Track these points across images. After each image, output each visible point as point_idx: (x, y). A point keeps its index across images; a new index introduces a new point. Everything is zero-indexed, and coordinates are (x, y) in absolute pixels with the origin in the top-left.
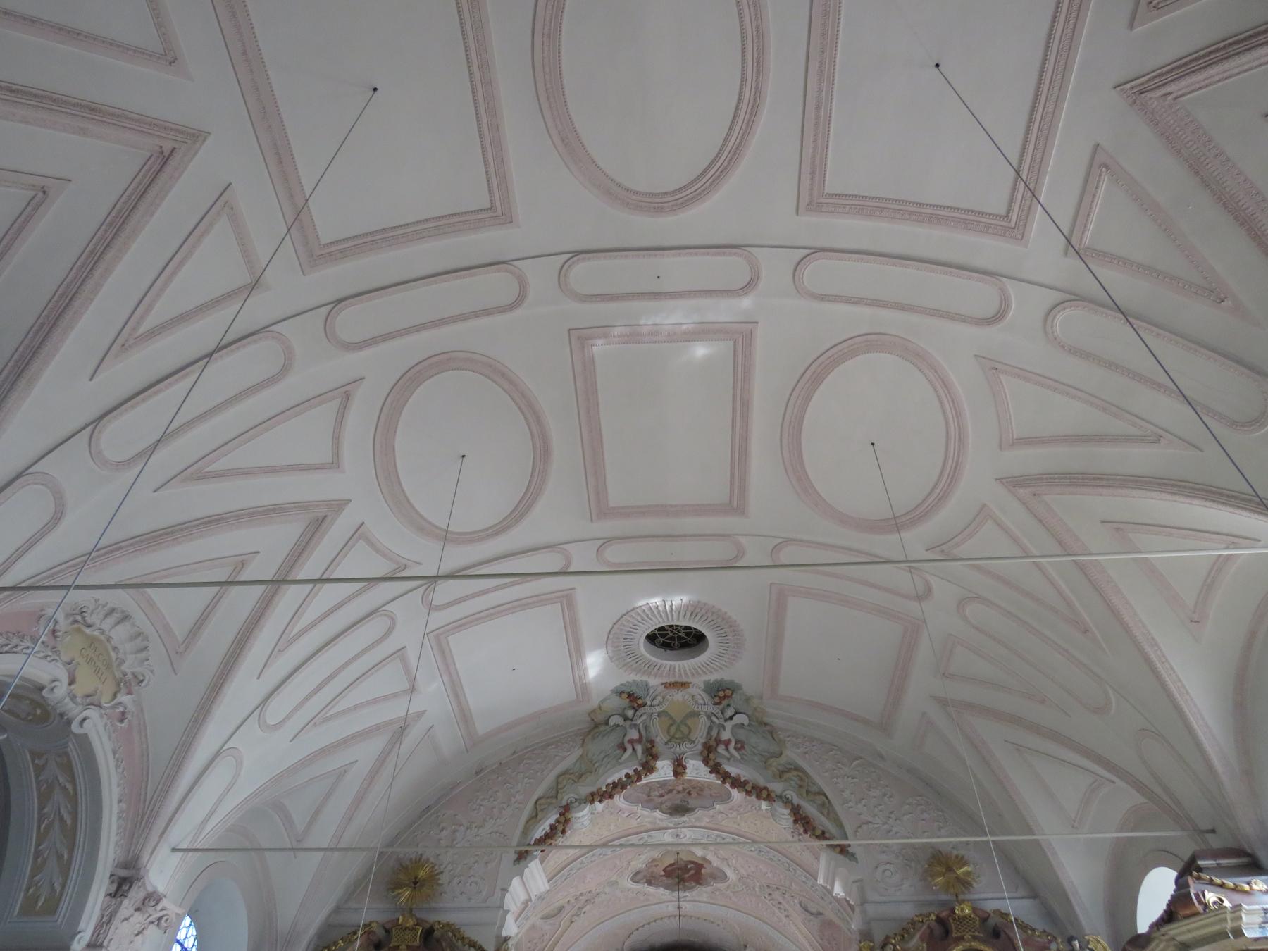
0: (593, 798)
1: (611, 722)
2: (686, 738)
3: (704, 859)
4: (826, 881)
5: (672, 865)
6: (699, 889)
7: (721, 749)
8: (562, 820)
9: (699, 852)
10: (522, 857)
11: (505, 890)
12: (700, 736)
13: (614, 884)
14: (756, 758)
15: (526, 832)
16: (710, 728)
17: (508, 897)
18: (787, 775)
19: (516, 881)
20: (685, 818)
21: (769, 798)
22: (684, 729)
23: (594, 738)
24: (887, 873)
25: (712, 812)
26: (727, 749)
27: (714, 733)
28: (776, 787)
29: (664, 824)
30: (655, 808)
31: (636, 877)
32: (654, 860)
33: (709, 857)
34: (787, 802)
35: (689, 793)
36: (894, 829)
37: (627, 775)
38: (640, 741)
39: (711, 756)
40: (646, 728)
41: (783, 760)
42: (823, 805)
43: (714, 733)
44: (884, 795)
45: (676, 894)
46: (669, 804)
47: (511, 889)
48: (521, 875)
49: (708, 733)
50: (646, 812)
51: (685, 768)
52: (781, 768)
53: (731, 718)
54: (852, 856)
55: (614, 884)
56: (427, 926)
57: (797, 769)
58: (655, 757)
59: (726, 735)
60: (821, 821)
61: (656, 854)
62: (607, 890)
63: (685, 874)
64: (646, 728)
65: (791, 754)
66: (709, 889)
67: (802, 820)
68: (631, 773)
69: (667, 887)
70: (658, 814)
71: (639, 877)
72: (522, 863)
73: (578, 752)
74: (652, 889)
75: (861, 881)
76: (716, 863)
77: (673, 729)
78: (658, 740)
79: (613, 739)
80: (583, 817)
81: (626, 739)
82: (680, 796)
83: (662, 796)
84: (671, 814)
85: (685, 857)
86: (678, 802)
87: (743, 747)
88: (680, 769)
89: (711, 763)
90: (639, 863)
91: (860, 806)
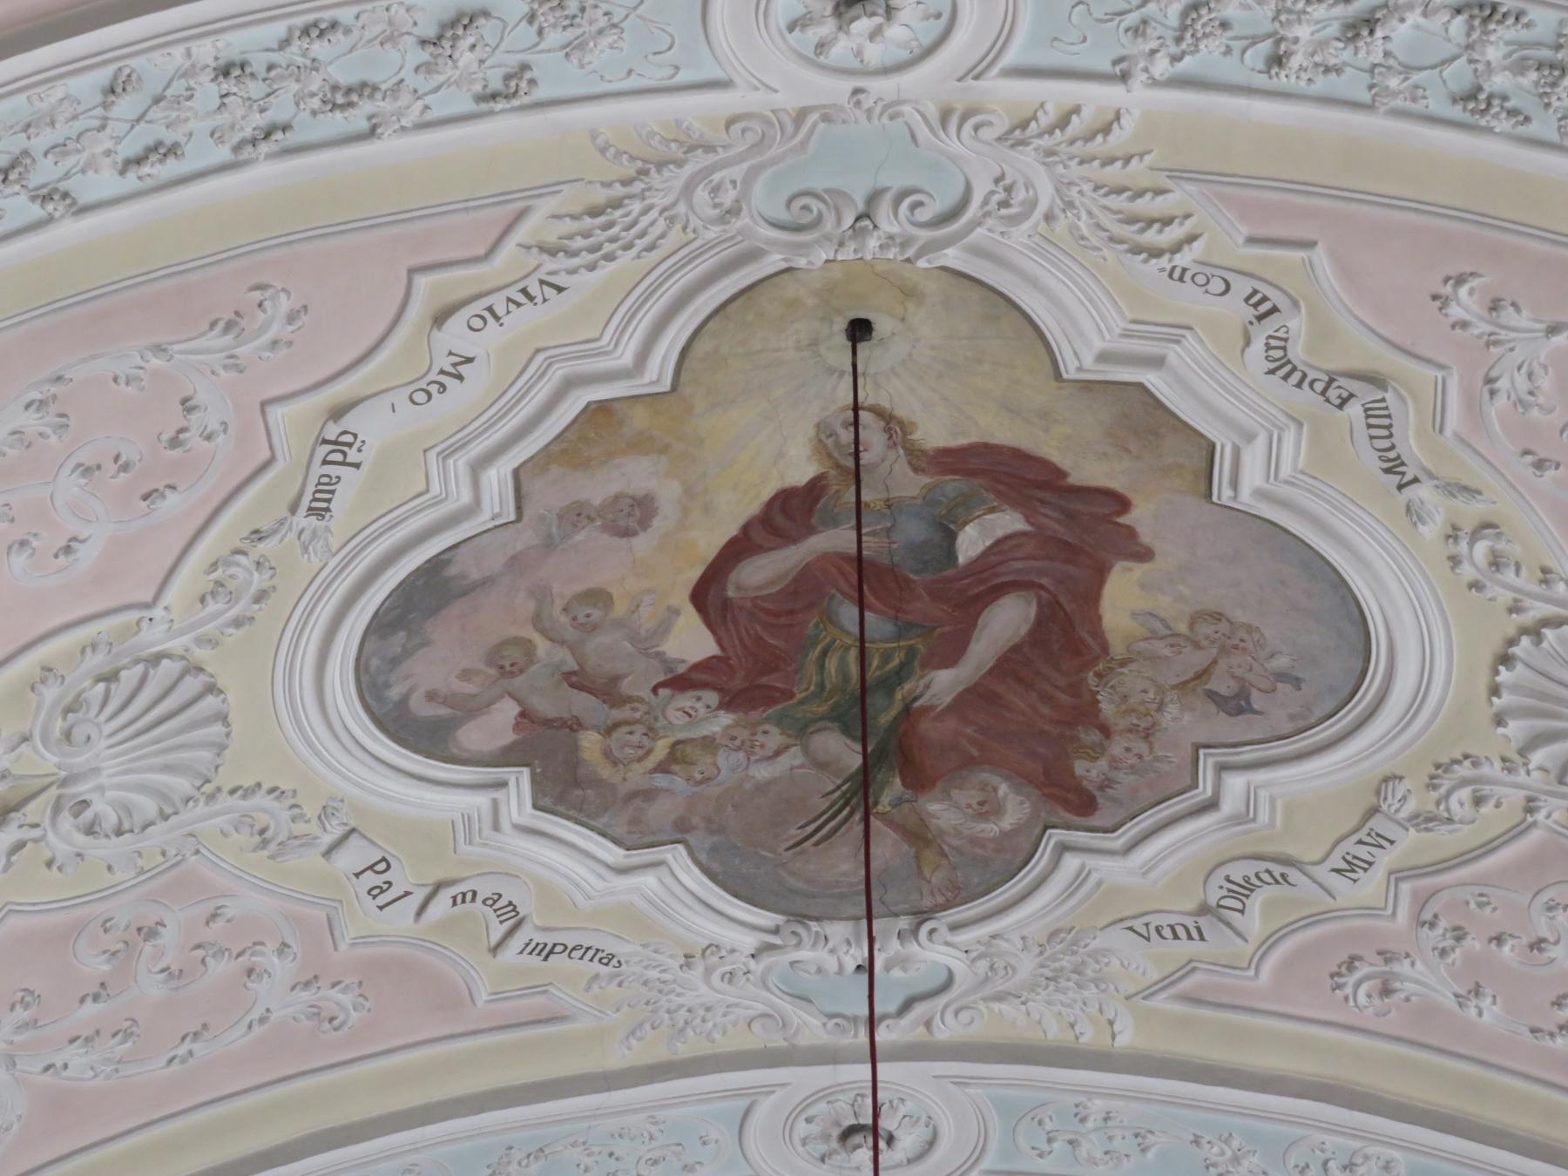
3: (1143, 418)
5: (790, 512)
9: (1087, 322)
13: (175, 698)
33: (1207, 383)
45: (834, 949)
55: (175, 698)
61: (620, 336)
62: (113, 773)
66: (1153, 862)
71: (436, 668)
74: (569, 865)
76: (1271, 458)
90: (440, 467)
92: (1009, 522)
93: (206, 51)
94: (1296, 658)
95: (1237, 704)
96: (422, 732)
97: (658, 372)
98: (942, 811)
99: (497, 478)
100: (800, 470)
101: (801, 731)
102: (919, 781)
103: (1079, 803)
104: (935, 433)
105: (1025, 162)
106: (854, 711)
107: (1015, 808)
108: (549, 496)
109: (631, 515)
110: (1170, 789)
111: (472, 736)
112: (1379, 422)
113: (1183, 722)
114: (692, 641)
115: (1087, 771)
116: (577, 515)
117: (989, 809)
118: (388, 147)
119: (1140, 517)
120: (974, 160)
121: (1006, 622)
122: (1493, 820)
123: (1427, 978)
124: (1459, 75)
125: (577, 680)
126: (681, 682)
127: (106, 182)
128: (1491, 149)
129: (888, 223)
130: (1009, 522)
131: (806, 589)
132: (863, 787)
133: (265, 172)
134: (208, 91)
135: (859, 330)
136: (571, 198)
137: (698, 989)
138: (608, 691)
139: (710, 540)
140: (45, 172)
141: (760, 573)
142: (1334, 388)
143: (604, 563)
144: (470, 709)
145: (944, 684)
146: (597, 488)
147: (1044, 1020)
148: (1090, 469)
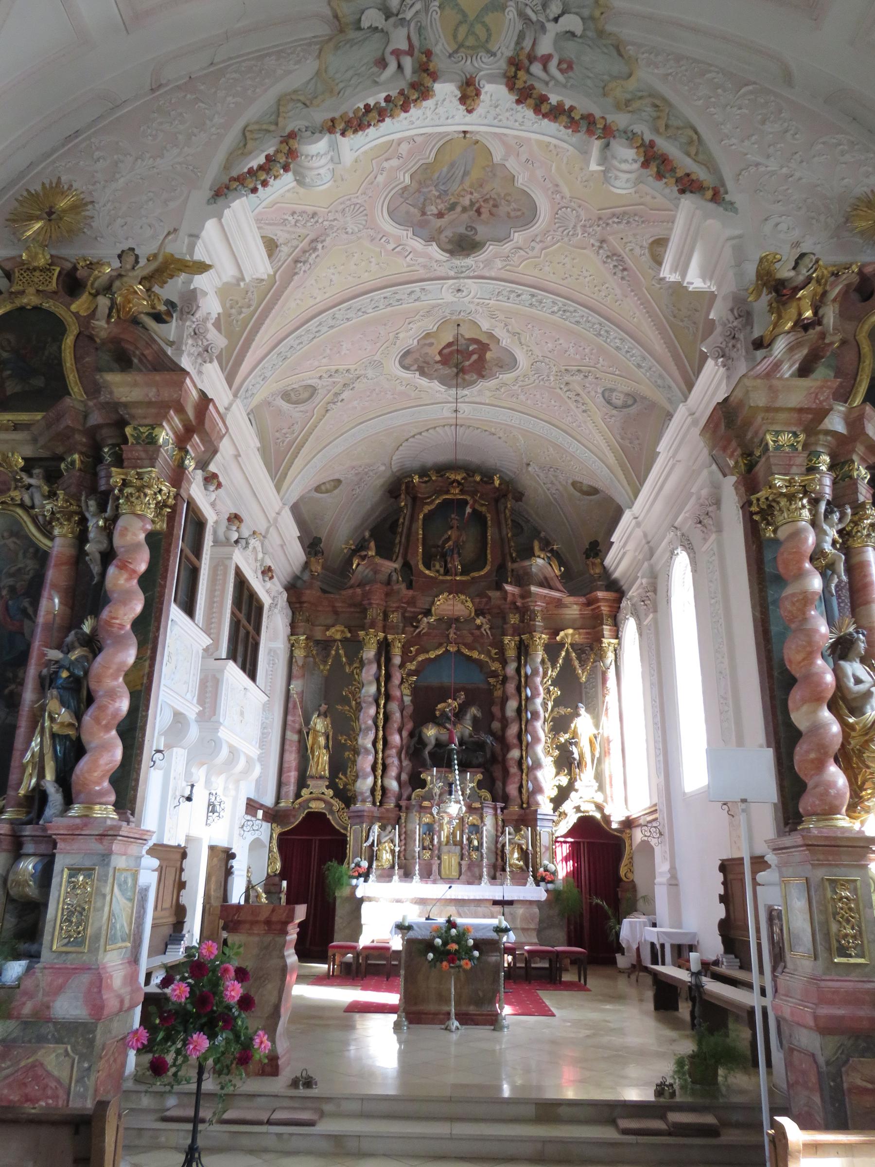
0: (330, 127)
1: (365, 24)
2: (483, 46)
3: (491, 336)
4: (674, 269)
5: (450, 345)
6: (482, 384)
7: (536, 69)
8: (285, 149)
9: (485, 325)
10: (222, 192)
11: (195, 237)
12: (505, 46)
14: (589, 82)
15: (227, 165)
16: (521, 36)
17: (200, 243)
18: (636, 105)
19: (211, 227)
20: (469, 261)
21: (608, 133)
22: (479, 29)
23: (337, 48)
24: (783, 227)
25: (507, 247)
26: (545, 69)
27: (527, 44)
28: (620, 120)
29: (442, 271)
30: (430, 239)
31: (407, 360)
32: (428, 335)
33: (498, 333)
34: (631, 137)
35: (479, 212)
36: (797, 175)
37: (388, 99)
38: (410, 52)
39: (521, 74)
40: (420, 30)
41: (632, 84)
42: (691, 142)
43: (527, 44)
44: (786, 131)
45: (453, 391)
46: (449, 233)
47: (204, 234)
48: (220, 216)
49: (518, 43)
50: (417, 244)
51: (478, 94)
52: (629, 96)
53: (556, 20)
54: (731, 206)
56: (69, 266)
57: (653, 94)
58: (434, 76)
59: (545, 46)
60: (685, 163)
62: (370, 373)
63: (464, 359)
64: (420, 30)
65: (647, 76)
66: (492, 383)
67: (654, 160)
68: (394, 93)
69: (443, 382)
70: (434, 250)
71: (408, 361)
72: (221, 201)
73: (310, 66)
74: (424, 382)
75: (740, 237)
76: (506, 341)
77: (463, 30)
78: (437, 50)
79: (371, 49)
80: (317, 150)
81: (390, 49)
82: (465, 216)
83: (440, 215)
84: (451, 252)
85: (467, 333)
86: (462, 230)
87: (570, 67)
88: (470, 91)
89: (519, 84)
90: (409, 339)
91: (746, 143)
92: (475, 346)
93: (382, 296)
94: (508, 363)
95: (501, 367)
96: (406, 368)
97: (435, 329)
98: (467, 377)
99: (415, 341)
100: (451, 340)
101: (450, 368)
102: (464, 373)
103: (483, 377)
104: (467, 337)
105: (478, 308)
106: (456, 366)
107: (475, 377)
108: (422, 342)
109: (431, 344)
110: (493, 376)
111: (412, 368)
112: (519, 339)
113: (495, 369)
114: (438, 358)
115: (484, 373)
116: (425, 344)
117: (472, 377)
118: (404, 306)
119: (491, 346)
120: (472, 307)
121: (475, 357)
122: (530, 382)
123: (522, 397)
124: (529, 302)
125: (425, 362)
126: (437, 362)
127: (371, 310)
128: (533, 310)
129: (462, 314)
130: (475, 346)
131: (451, 353)
132: (457, 374)
133: (389, 309)
134: (383, 300)
135: (458, 325)
136: (425, 310)
137: (438, 395)
138: (428, 363)
139: (441, 347)
140: (363, 310)
141: (446, 351)
142: (514, 334)
143: (427, 350)
144: (412, 365)
145: (467, 363)
146: (428, 342)
147: (477, 399)
148: (485, 341)
